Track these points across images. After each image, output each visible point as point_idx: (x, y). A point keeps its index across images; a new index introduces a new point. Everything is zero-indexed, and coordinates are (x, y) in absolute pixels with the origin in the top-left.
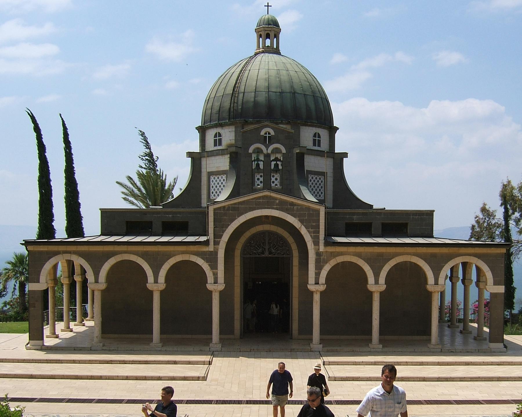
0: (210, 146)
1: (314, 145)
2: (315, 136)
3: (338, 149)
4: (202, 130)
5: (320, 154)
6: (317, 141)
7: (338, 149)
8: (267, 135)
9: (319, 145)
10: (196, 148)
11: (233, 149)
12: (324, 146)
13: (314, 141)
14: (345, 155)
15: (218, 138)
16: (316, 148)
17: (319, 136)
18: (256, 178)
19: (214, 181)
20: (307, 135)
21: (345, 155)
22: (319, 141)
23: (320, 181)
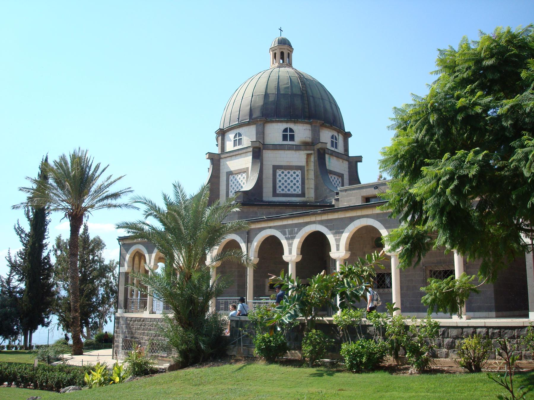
0: (230, 146)
1: (332, 146)
2: (332, 137)
3: (351, 154)
4: (222, 133)
5: (338, 155)
6: (334, 144)
7: (351, 154)
8: (288, 133)
9: (336, 148)
10: (216, 150)
11: (257, 145)
12: (340, 149)
13: (332, 142)
14: (359, 159)
15: (238, 138)
16: (333, 149)
17: (336, 139)
18: (278, 175)
19: (234, 180)
20: (326, 136)
21: (359, 159)
22: (336, 143)
23: (338, 182)
